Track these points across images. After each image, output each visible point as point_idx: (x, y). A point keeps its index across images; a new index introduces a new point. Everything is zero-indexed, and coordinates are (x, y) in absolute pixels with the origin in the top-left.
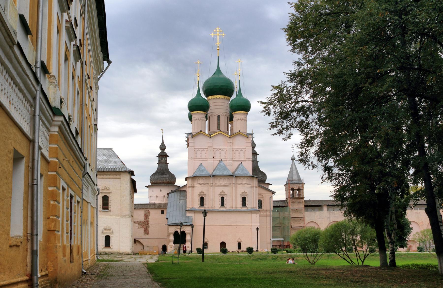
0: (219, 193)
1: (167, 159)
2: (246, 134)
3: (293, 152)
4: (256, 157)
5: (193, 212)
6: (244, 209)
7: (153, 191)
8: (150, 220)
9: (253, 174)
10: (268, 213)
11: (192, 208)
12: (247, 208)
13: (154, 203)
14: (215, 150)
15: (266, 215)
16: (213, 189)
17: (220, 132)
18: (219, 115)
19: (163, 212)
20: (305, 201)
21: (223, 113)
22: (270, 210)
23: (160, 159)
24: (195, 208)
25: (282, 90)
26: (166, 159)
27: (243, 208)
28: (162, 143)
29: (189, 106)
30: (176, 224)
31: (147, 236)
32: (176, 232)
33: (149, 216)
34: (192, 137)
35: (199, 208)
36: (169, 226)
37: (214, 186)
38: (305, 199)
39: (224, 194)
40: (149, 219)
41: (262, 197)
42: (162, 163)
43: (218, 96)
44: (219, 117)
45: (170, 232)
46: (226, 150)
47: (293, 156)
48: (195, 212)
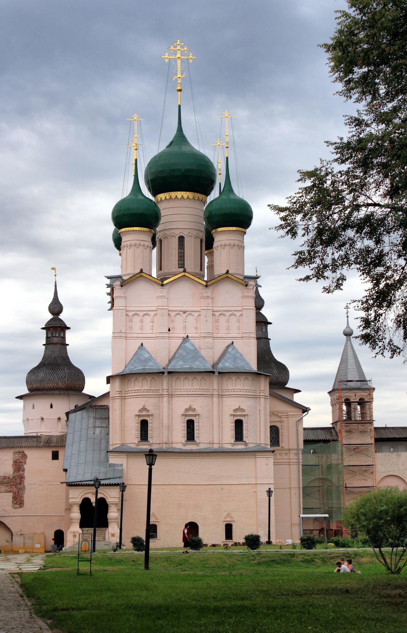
0: (182, 411)
1: (64, 335)
2: (242, 278)
3: (348, 317)
4: (264, 330)
5: (125, 456)
6: (240, 447)
7: (34, 408)
8: (26, 474)
9: (258, 368)
10: (292, 456)
11: (122, 444)
12: (246, 444)
13: (35, 434)
14: (173, 314)
15: (288, 461)
16: (169, 402)
17: (183, 274)
19: (55, 456)
20: (376, 428)
21: (192, 231)
22: (298, 449)
23: (49, 335)
24: (129, 445)
25: (322, 180)
26: (62, 335)
27: (237, 444)
28: (54, 299)
29: (115, 215)
30: (85, 483)
31: (20, 512)
32: (86, 502)
33: (25, 463)
34: (122, 286)
35: (138, 445)
36: (70, 488)
37: (171, 396)
38: (376, 424)
39: (193, 413)
40: (24, 470)
41: (279, 419)
42: (53, 344)
43: (179, 194)
44: (181, 239)
45: (71, 500)
46: (197, 314)
47: (347, 328)
48: (129, 454)
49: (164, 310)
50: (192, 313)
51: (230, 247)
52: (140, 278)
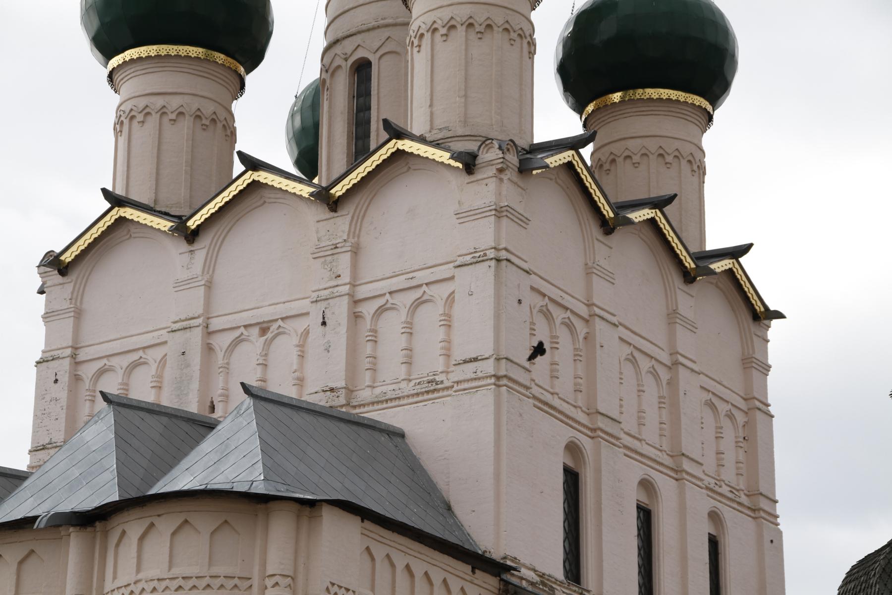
18: (360, 54)
49: (188, 334)
50: (288, 325)
51: (438, 35)
52: (121, 232)
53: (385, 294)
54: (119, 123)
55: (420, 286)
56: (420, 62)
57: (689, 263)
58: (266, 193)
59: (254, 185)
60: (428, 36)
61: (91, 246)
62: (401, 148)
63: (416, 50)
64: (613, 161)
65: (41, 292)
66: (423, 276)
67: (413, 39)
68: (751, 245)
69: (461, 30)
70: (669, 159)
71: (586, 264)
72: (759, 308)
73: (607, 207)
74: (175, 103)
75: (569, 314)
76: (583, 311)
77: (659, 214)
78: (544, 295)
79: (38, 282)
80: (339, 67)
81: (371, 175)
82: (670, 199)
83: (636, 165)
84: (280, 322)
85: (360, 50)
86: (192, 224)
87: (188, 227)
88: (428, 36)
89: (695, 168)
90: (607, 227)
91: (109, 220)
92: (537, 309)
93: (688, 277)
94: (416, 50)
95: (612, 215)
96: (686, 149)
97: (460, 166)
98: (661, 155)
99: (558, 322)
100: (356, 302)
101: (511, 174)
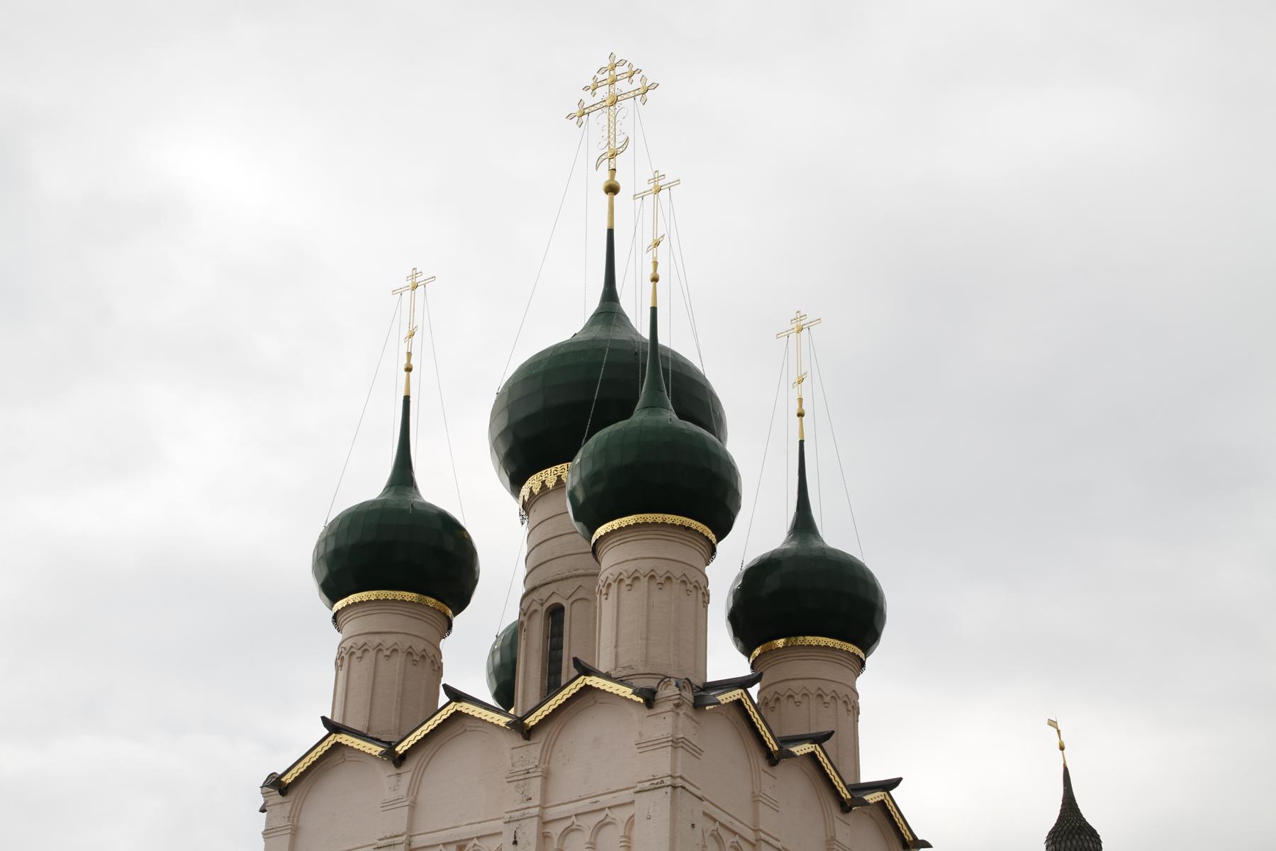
51: (623, 586)
52: (337, 756)
53: (571, 817)
54: (340, 658)
55: (602, 809)
56: (607, 608)
57: (846, 794)
58: (467, 722)
59: (457, 715)
60: (614, 586)
61: (309, 769)
62: (589, 683)
63: (603, 597)
64: (778, 700)
65: (263, 810)
66: (606, 800)
67: (601, 588)
68: (900, 780)
69: (644, 581)
70: (827, 699)
71: (753, 793)
72: (908, 837)
73: (772, 741)
74: (389, 641)
75: (737, 838)
76: (750, 835)
77: (818, 748)
78: (715, 820)
79: (261, 801)
80: (536, 611)
81: (561, 707)
82: (828, 736)
83: (798, 704)
84: (475, 841)
85: (555, 595)
86: (400, 749)
87: (397, 752)
88: (614, 586)
89: (850, 708)
90: (773, 759)
91: (326, 746)
92: (709, 833)
93: (845, 807)
94: (603, 597)
95: (776, 748)
96: (842, 691)
97: (641, 700)
98: (820, 696)
99: (728, 845)
100: (545, 823)
101: (686, 709)
